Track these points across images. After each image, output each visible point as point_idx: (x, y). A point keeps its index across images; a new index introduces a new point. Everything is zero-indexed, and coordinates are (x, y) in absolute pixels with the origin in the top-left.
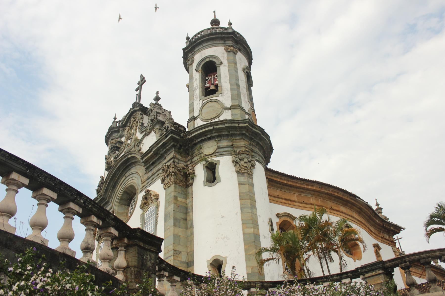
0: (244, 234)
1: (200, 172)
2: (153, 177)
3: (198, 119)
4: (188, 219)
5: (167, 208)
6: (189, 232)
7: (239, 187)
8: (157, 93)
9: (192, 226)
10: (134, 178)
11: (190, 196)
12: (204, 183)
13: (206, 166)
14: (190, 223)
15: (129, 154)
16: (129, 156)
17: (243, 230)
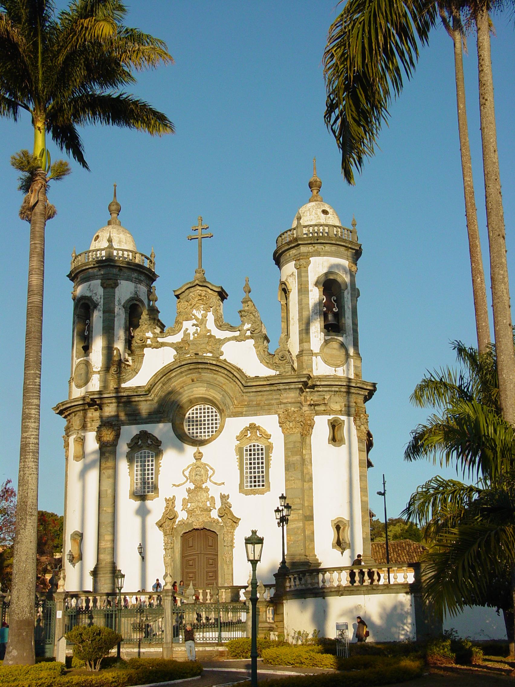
0: (361, 501)
1: (321, 425)
2: (259, 408)
3: (319, 357)
4: (305, 471)
5: (289, 457)
6: (306, 485)
7: (359, 454)
8: (247, 281)
9: (311, 480)
10: (211, 390)
11: (308, 448)
12: (329, 441)
13: (331, 423)
14: (307, 477)
15: (214, 360)
16: (214, 363)
17: (361, 497)
